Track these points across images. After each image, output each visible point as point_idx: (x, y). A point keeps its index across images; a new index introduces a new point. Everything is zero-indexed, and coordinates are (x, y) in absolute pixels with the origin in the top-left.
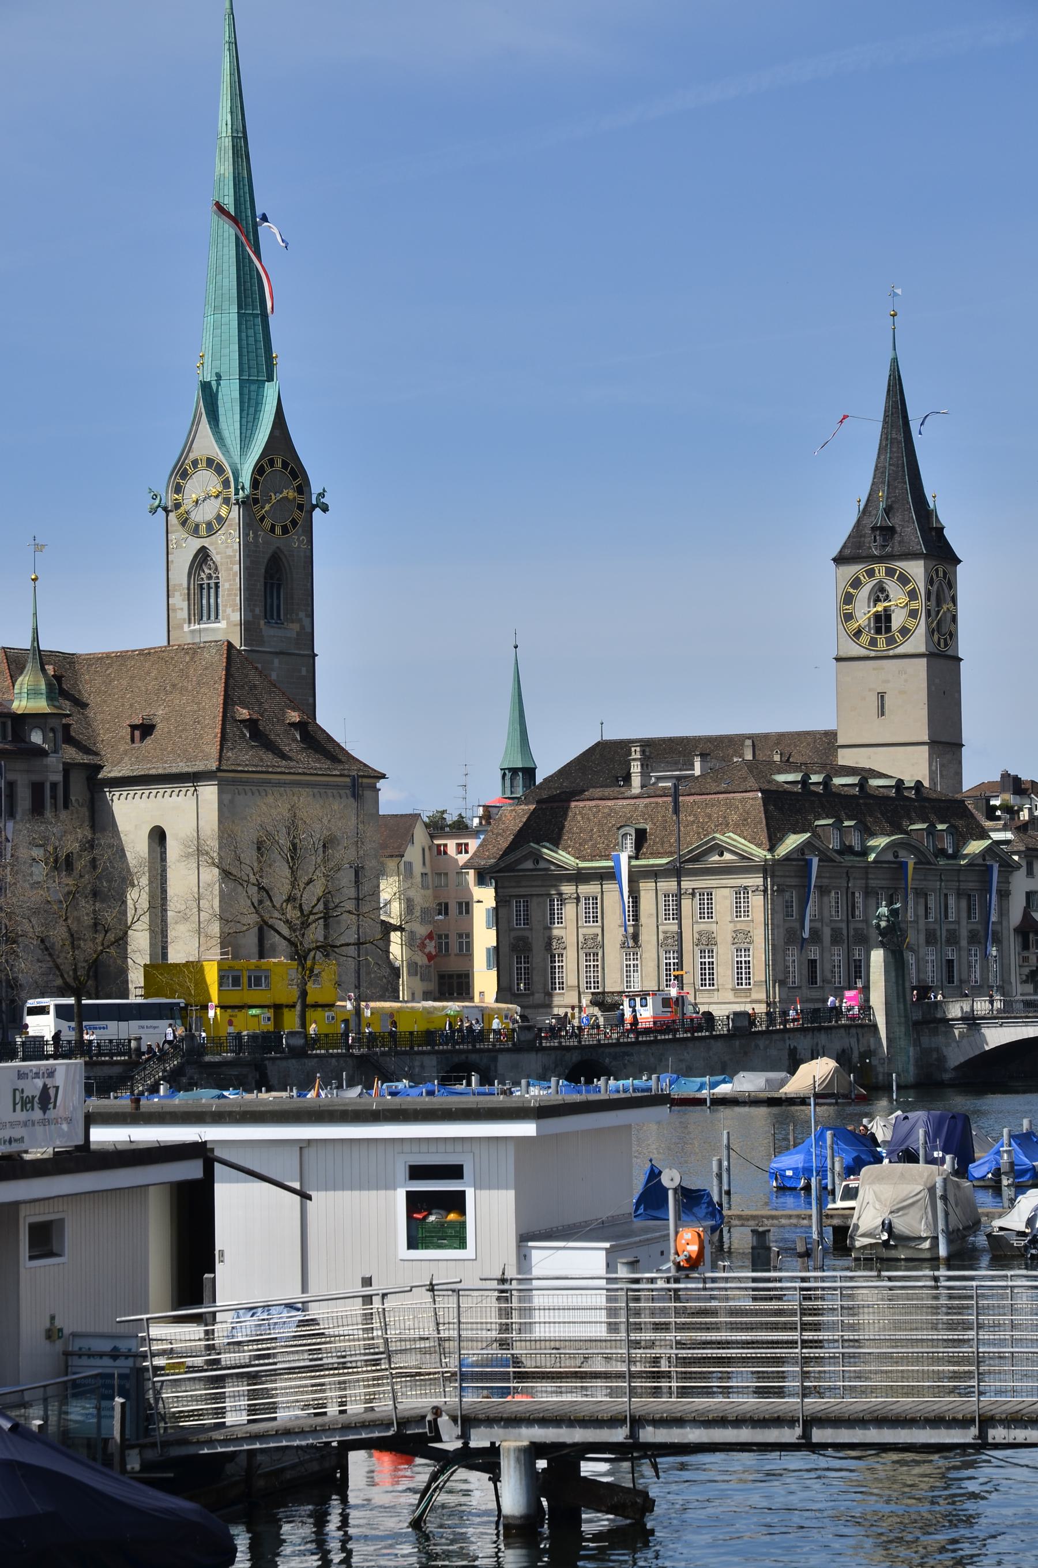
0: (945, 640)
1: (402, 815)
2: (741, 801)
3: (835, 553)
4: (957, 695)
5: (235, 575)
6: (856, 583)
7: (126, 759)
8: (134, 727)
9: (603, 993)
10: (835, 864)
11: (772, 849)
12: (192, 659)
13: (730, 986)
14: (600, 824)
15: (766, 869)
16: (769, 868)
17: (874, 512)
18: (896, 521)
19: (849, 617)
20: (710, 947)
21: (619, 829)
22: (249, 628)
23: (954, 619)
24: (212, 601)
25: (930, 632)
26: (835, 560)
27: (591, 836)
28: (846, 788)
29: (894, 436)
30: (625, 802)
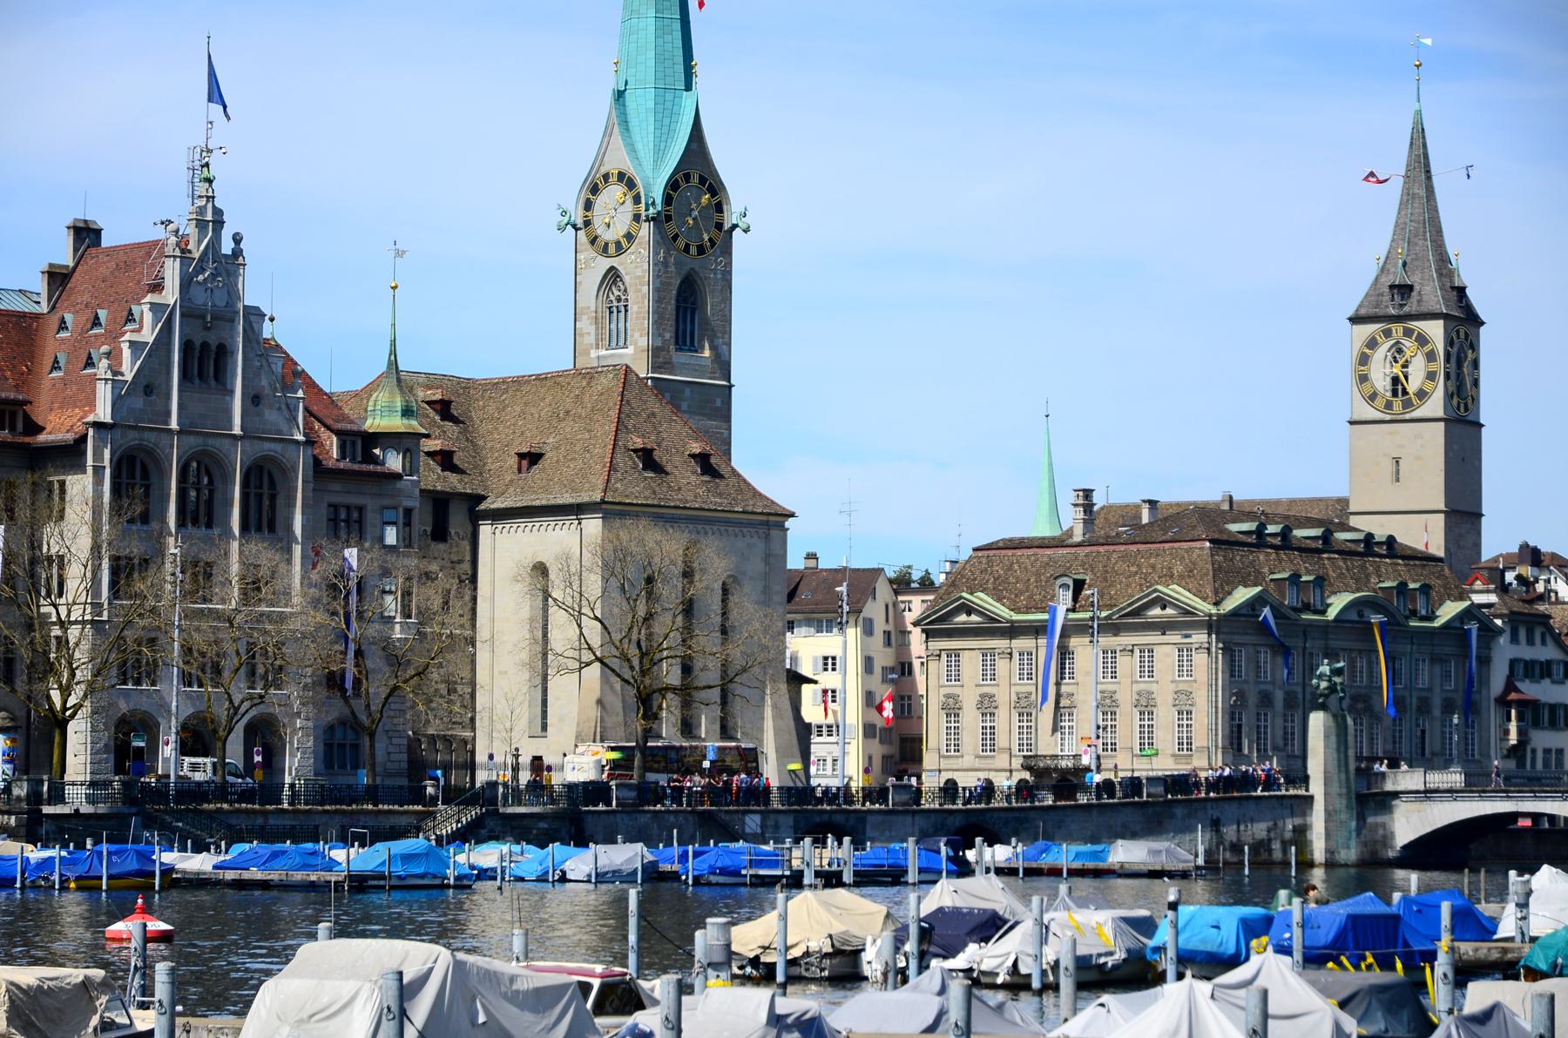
0: (1466, 405)
1: (864, 570)
2: (1187, 551)
3: (1351, 312)
4: (1477, 463)
5: (644, 296)
6: (1372, 344)
7: (512, 489)
8: (521, 456)
9: (1036, 756)
10: (1289, 622)
11: (1216, 604)
12: (589, 383)
13: (1170, 752)
14: (1038, 574)
15: (1213, 625)
16: (1214, 624)
17: (1392, 270)
18: (1414, 279)
19: (1363, 379)
20: (1149, 708)
21: (1055, 578)
22: (658, 358)
23: (1476, 383)
24: (621, 325)
25: (1449, 396)
26: (1351, 319)
27: (1028, 587)
28: (1308, 541)
29: (1416, 191)
30: (1065, 551)
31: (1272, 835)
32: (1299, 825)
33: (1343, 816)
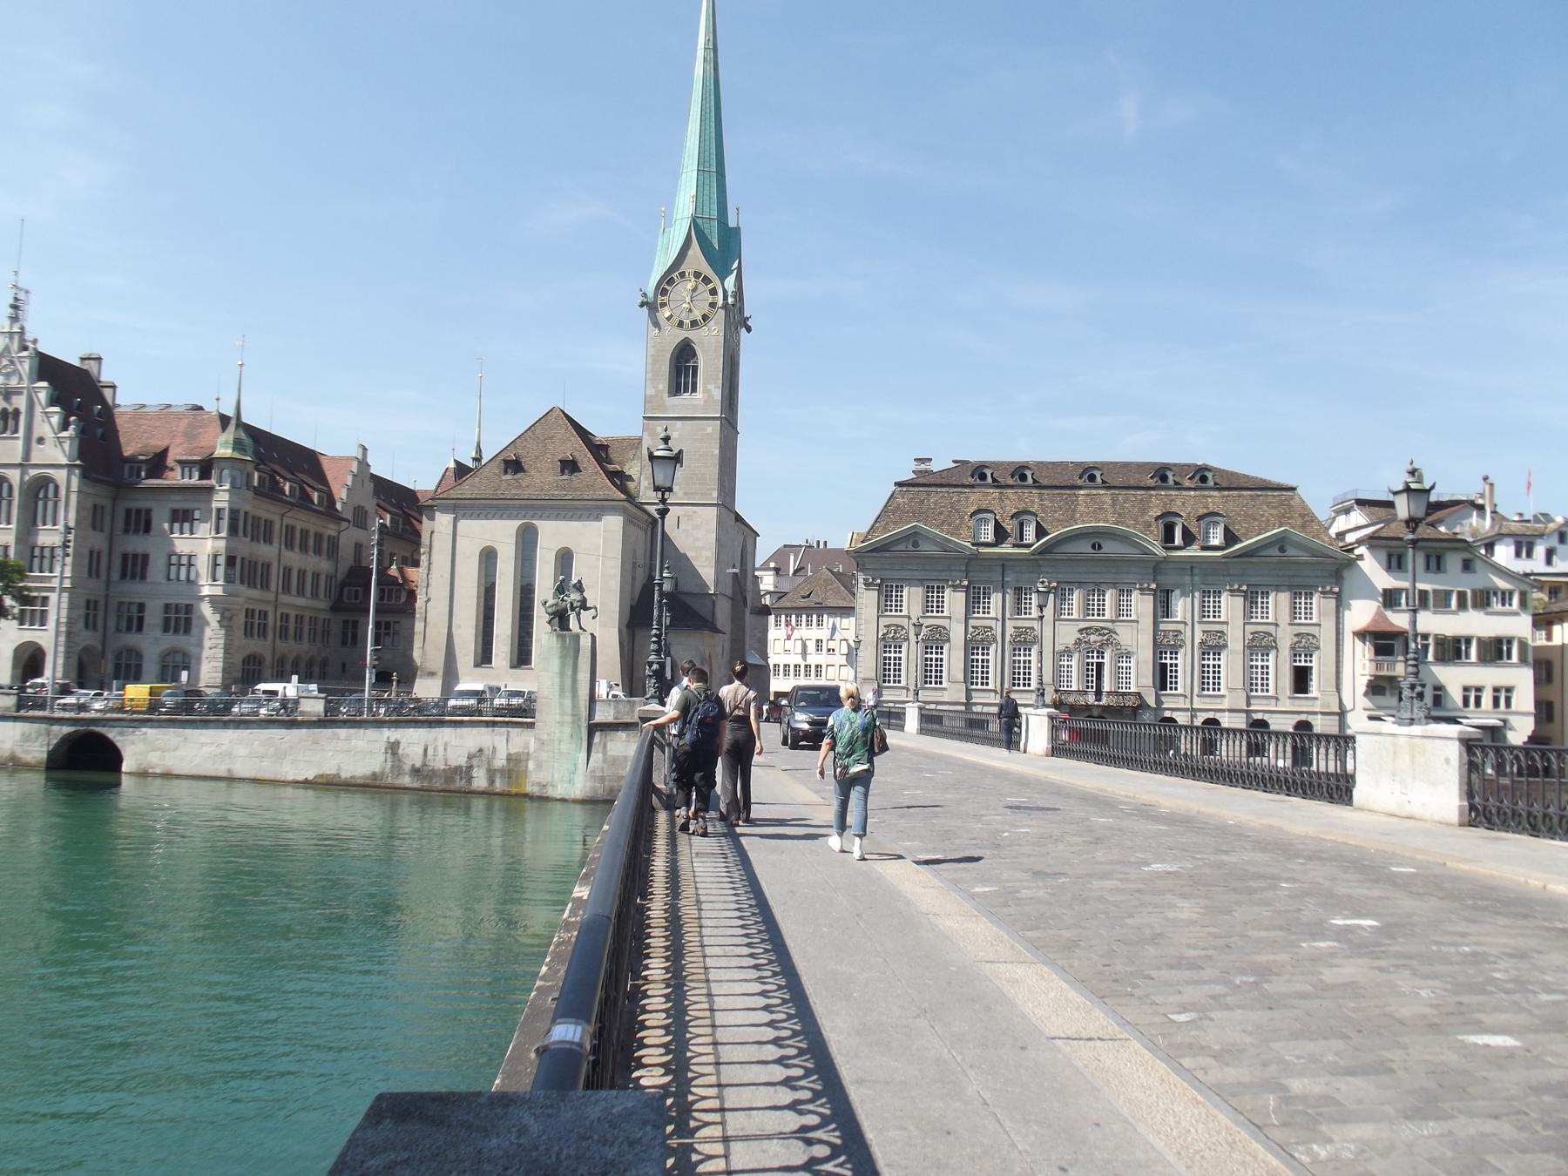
31: (475, 762)
32: (517, 754)
33: (565, 747)
